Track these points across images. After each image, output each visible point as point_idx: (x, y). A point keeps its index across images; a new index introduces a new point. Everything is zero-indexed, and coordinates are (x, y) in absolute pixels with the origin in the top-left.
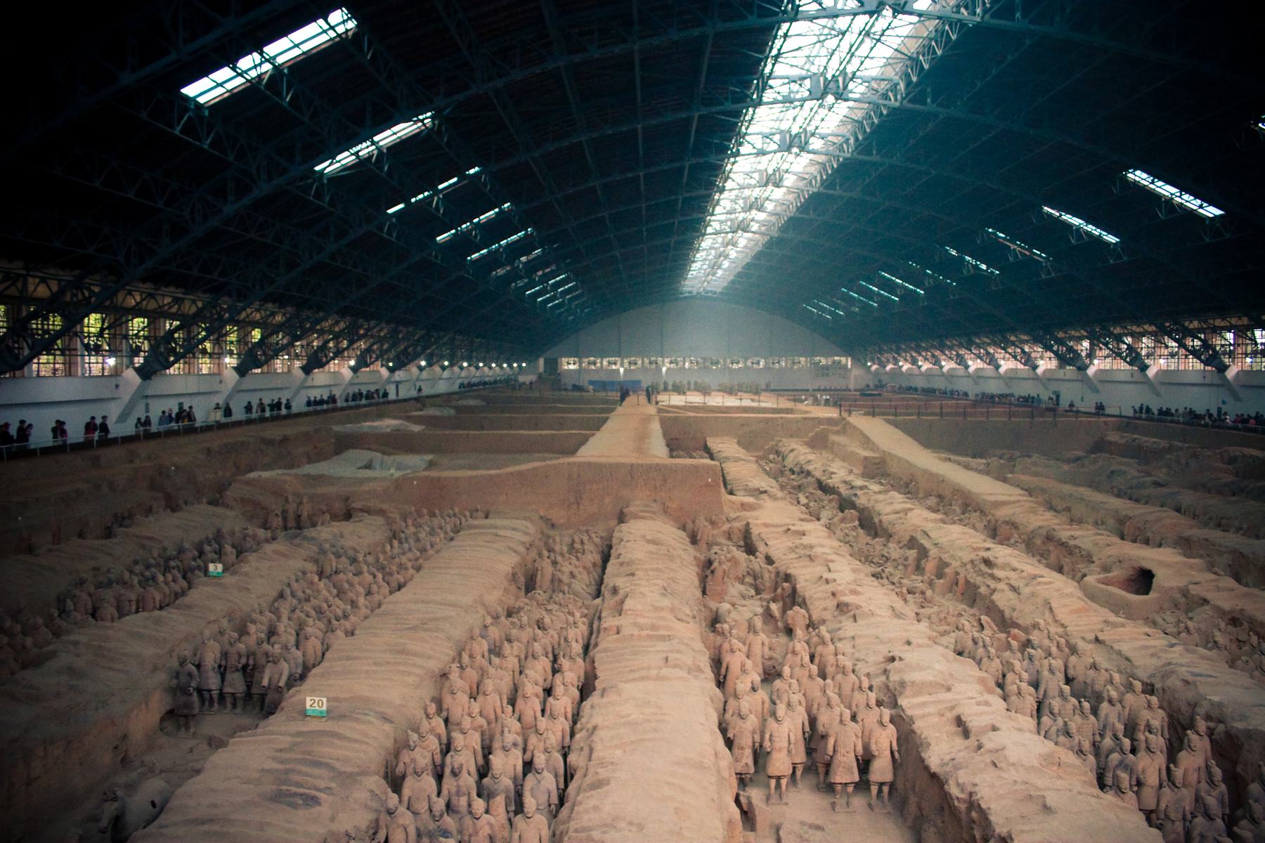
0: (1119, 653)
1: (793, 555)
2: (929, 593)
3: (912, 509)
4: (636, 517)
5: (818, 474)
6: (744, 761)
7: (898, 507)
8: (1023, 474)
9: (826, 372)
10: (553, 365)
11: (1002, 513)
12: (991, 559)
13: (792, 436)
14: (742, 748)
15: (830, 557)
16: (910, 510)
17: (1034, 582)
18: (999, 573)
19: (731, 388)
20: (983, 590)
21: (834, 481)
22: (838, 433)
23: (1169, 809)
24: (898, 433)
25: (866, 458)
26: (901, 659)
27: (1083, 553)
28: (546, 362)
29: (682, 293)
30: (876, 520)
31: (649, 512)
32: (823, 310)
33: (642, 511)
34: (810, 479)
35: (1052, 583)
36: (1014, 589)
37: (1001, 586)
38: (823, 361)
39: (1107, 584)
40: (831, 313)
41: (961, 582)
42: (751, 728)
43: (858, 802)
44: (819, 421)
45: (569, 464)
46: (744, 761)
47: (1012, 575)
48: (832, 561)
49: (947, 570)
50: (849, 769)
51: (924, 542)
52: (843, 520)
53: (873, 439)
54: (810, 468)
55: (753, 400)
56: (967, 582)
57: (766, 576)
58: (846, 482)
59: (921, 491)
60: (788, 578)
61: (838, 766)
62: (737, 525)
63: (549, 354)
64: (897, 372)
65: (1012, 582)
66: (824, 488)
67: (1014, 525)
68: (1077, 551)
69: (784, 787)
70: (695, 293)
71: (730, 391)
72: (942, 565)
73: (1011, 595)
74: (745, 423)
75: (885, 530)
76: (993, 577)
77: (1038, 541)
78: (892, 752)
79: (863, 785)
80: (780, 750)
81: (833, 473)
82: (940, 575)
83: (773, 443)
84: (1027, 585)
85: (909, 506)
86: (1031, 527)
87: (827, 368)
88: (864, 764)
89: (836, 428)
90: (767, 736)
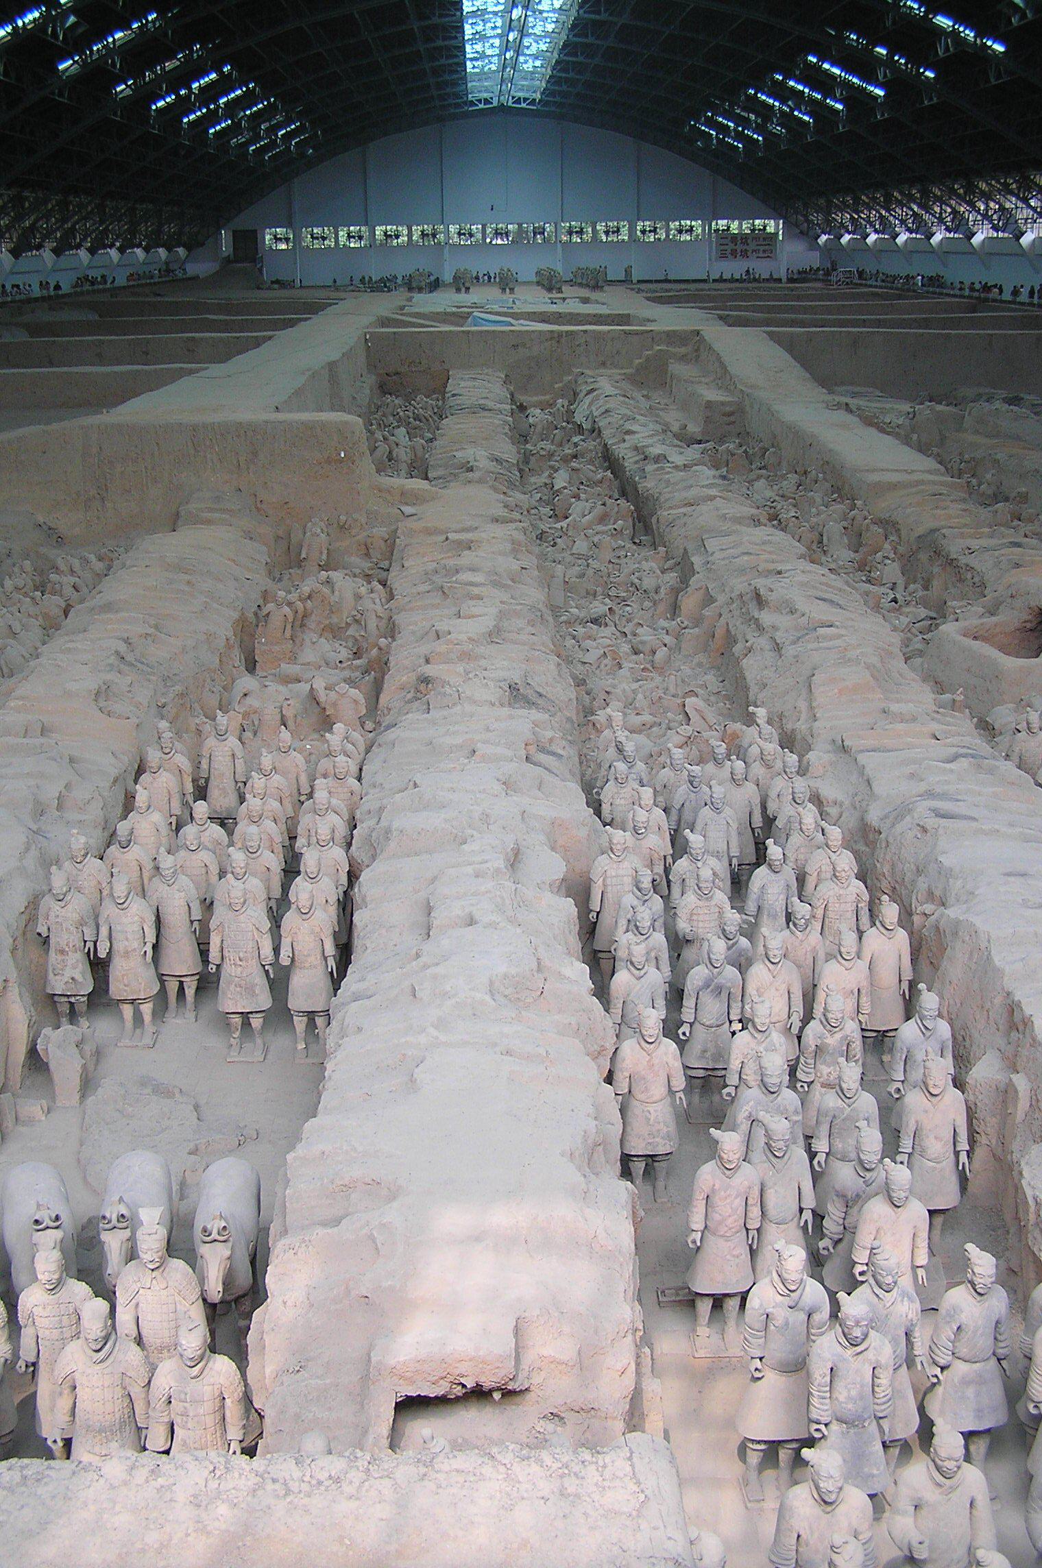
0: (861, 770)
1: (426, 587)
2: (662, 653)
3: (712, 498)
4: (196, 520)
5: (606, 433)
6: (68, 973)
7: (693, 492)
8: (977, 432)
9: (739, 247)
10: (248, 243)
11: (885, 506)
12: (762, 592)
13: (604, 364)
14: (62, 952)
15: (476, 591)
16: (712, 498)
17: (814, 634)
18: (766, 617)
19: (550, 279)
20: (738, 649)
21: (622, 451)
22: (683, 358)
23: (746, 1070)
24: (779, 355)
25: (709, 405)
26: (415, 785)
27: (976, 579)
28: (235, 233)
29: (472, 104)
30: (654, 520)
31: (223, 511)
32: (723, 129)
33: (211, 510)
34: (591, 444)
35: (840, 636)
36: (777, 648)
37: (763, 642)
38: (734, 226)
39: (975, 638)
40: (740, 136)
41: (720, 632)
42: (76, 916)
43: (280, 1042)
44: (653, 337)
45: (82, 427)
46: (68, 973)
47: (784, 621)
48: (480, 598)
49: (707, 612)
50: (250, 990)
51: (697, 560)
52: (602, 519)
53: (733, 369)
54: (602, 423)
55: (585, 301)
56: (728, 630)
57: (372, 624)
58: (636, 448)
59: (784, 464)
60: (392, 631)
61: (229, 983)
62: (381, 531)
63: (243, 221)
64: (860, 246)
65: (779, 636)
66: (610, 461)
67: (889, 525)
68: (969, 576)
69: (147, 1017)
70: (495, 104)
71: (549, 282)
72: (709, 600)
73: (770, 656)
74: (518, 341)
75: (662, 536)
76: (760, 628)
77: (923, 557)
78: (325, 959)
79: (279, 1014)
80: (127, 954)
81: (629, 432)
82: (697, 622)
83: (567, 378)
84: (794, 643)
85: (713, 492)
86: (921, 530)
87: (742, 238)
88: (279, 980)
89: (683, 350)
90: (104, 931)
